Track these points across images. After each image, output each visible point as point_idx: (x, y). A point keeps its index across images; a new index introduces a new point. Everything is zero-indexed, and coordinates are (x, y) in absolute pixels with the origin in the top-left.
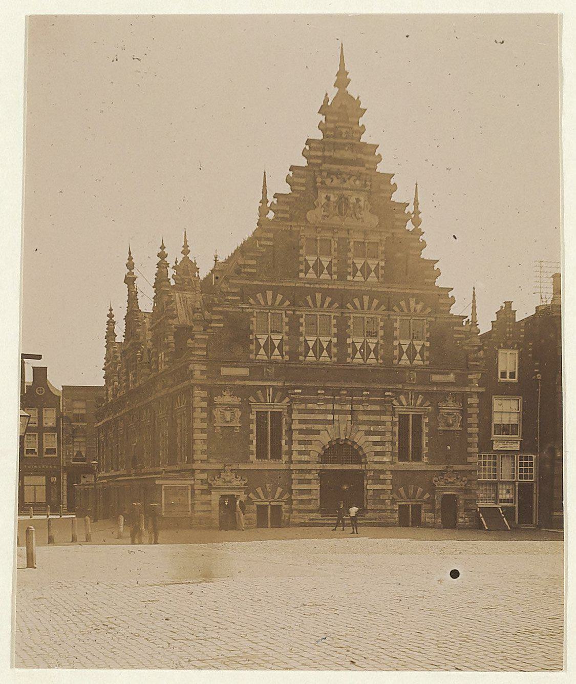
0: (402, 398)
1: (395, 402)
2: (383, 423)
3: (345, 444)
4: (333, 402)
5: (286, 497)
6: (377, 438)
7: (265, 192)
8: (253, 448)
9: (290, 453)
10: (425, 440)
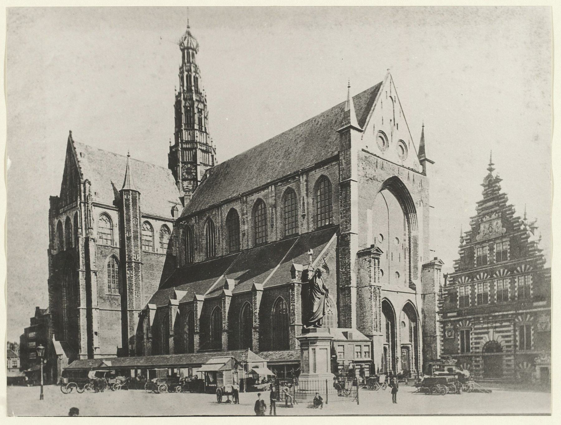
2: (509, 331)
4: (488, 323)
7: (461, 233)
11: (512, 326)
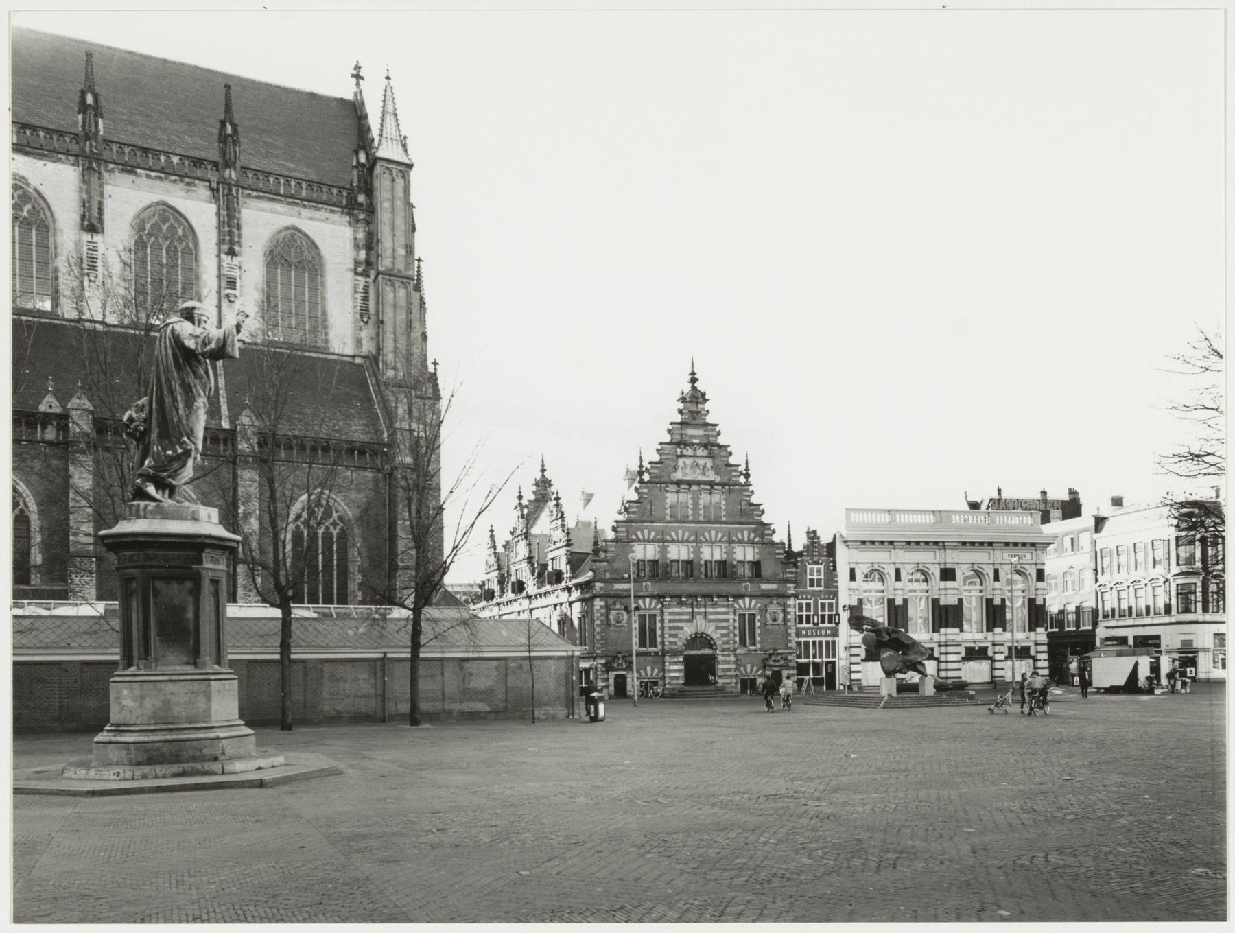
0: (741, 601)
1: (736, 606)
2: (727, 621)
3: (701, 636)
5: (662, 674)
6: (724, 632)
7: (641, 460)
8: (635, 640)
9: (663, 643)
10: (758, 631)
11: (731, 613)
